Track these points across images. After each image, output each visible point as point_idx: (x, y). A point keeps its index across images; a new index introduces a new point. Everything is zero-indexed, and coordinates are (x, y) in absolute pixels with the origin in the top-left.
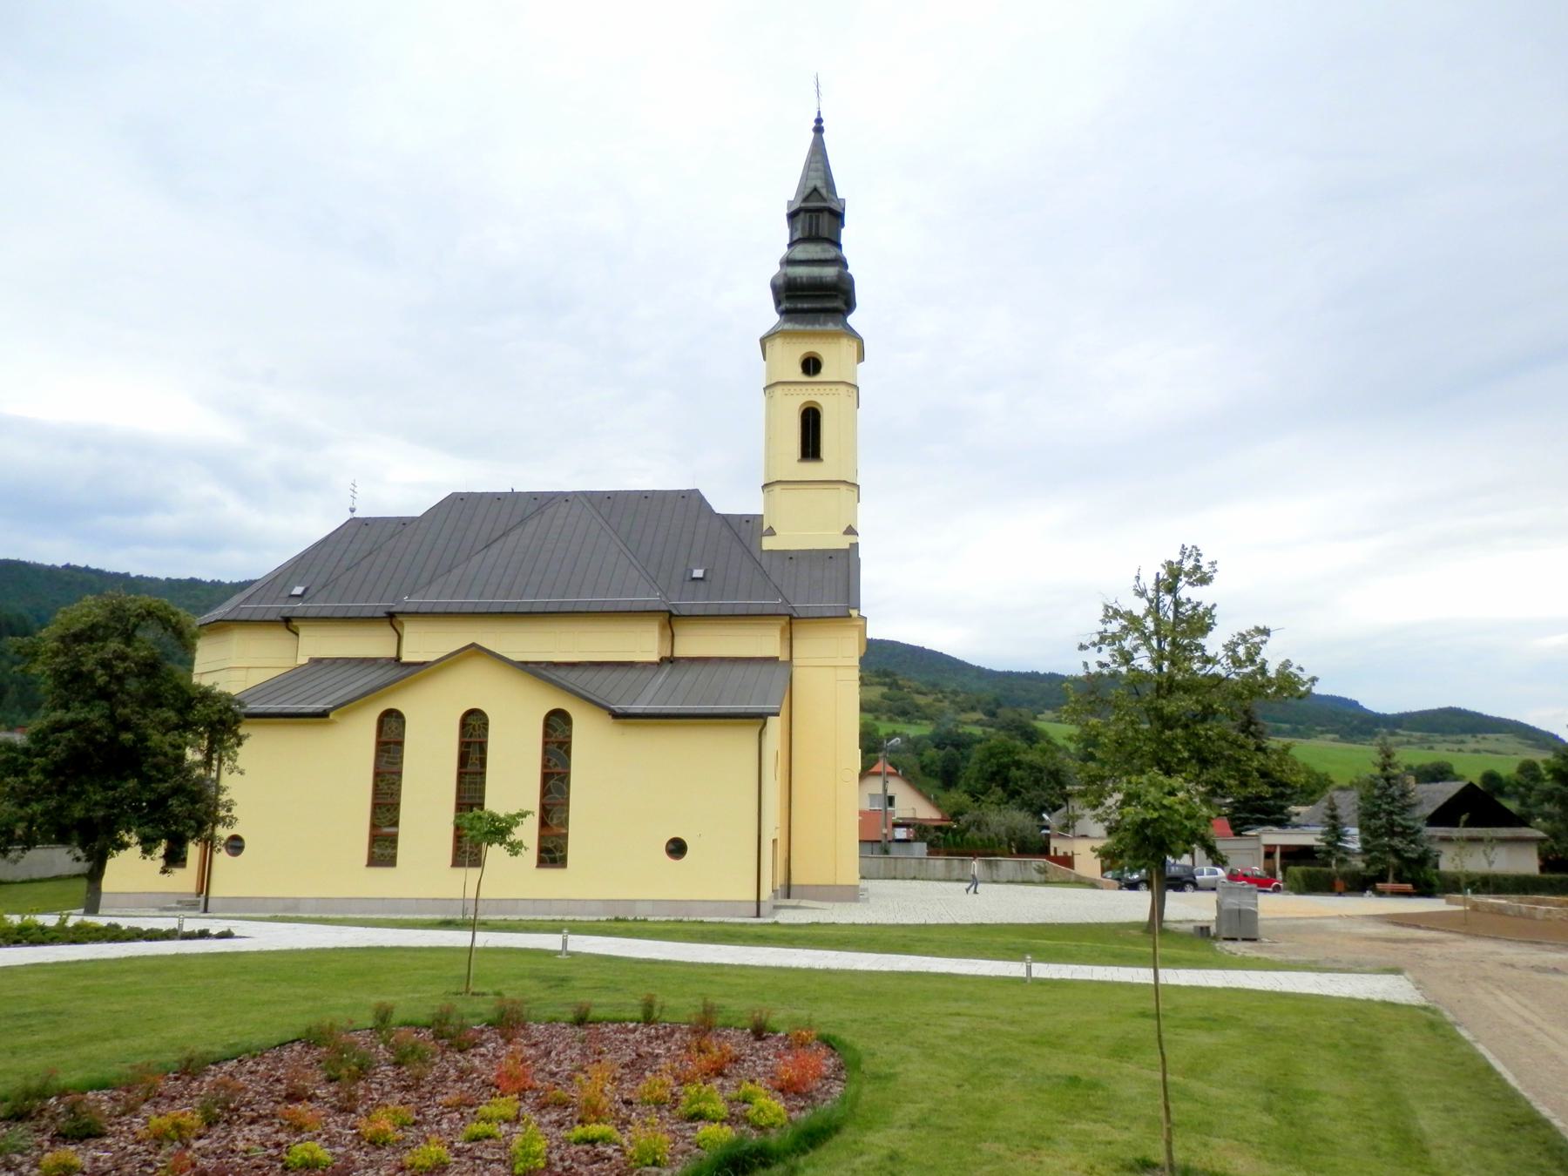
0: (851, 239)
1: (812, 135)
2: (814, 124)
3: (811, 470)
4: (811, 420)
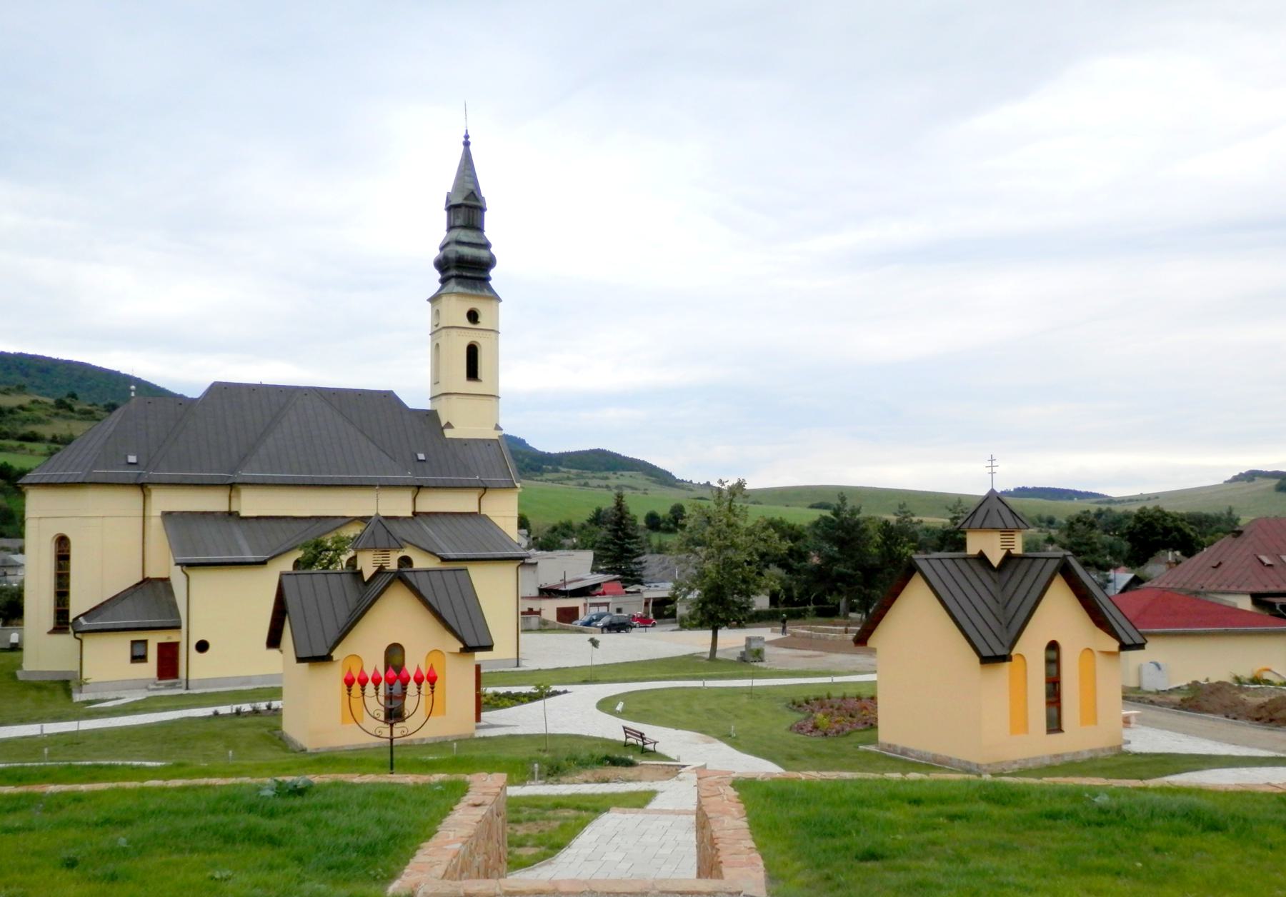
0: (493, 228)
1: (462, 147)
3: (473, 387)
4: (472, 352)
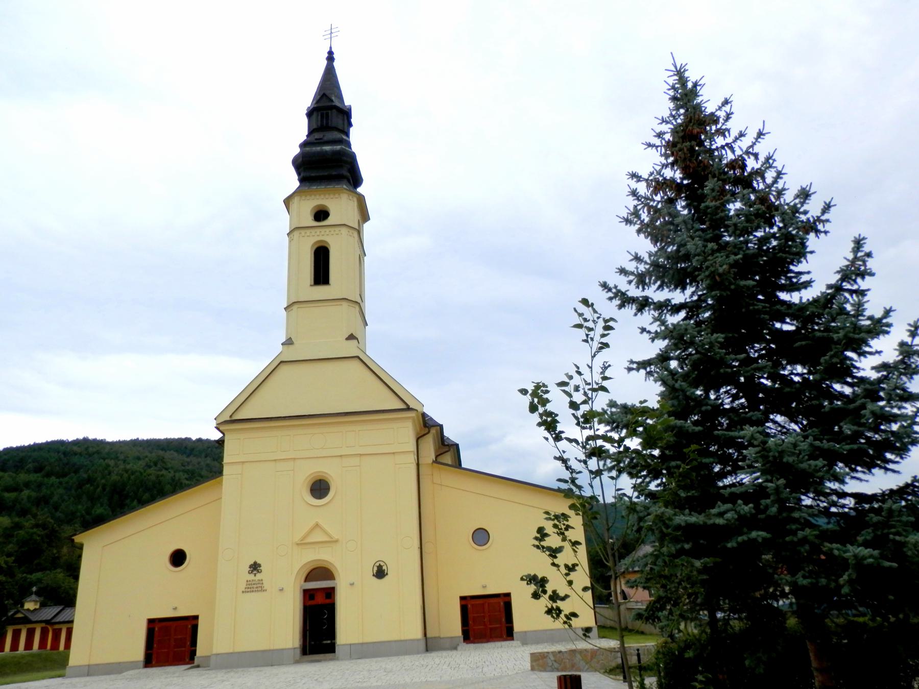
1: (325, 62)
2: (327, 55)
